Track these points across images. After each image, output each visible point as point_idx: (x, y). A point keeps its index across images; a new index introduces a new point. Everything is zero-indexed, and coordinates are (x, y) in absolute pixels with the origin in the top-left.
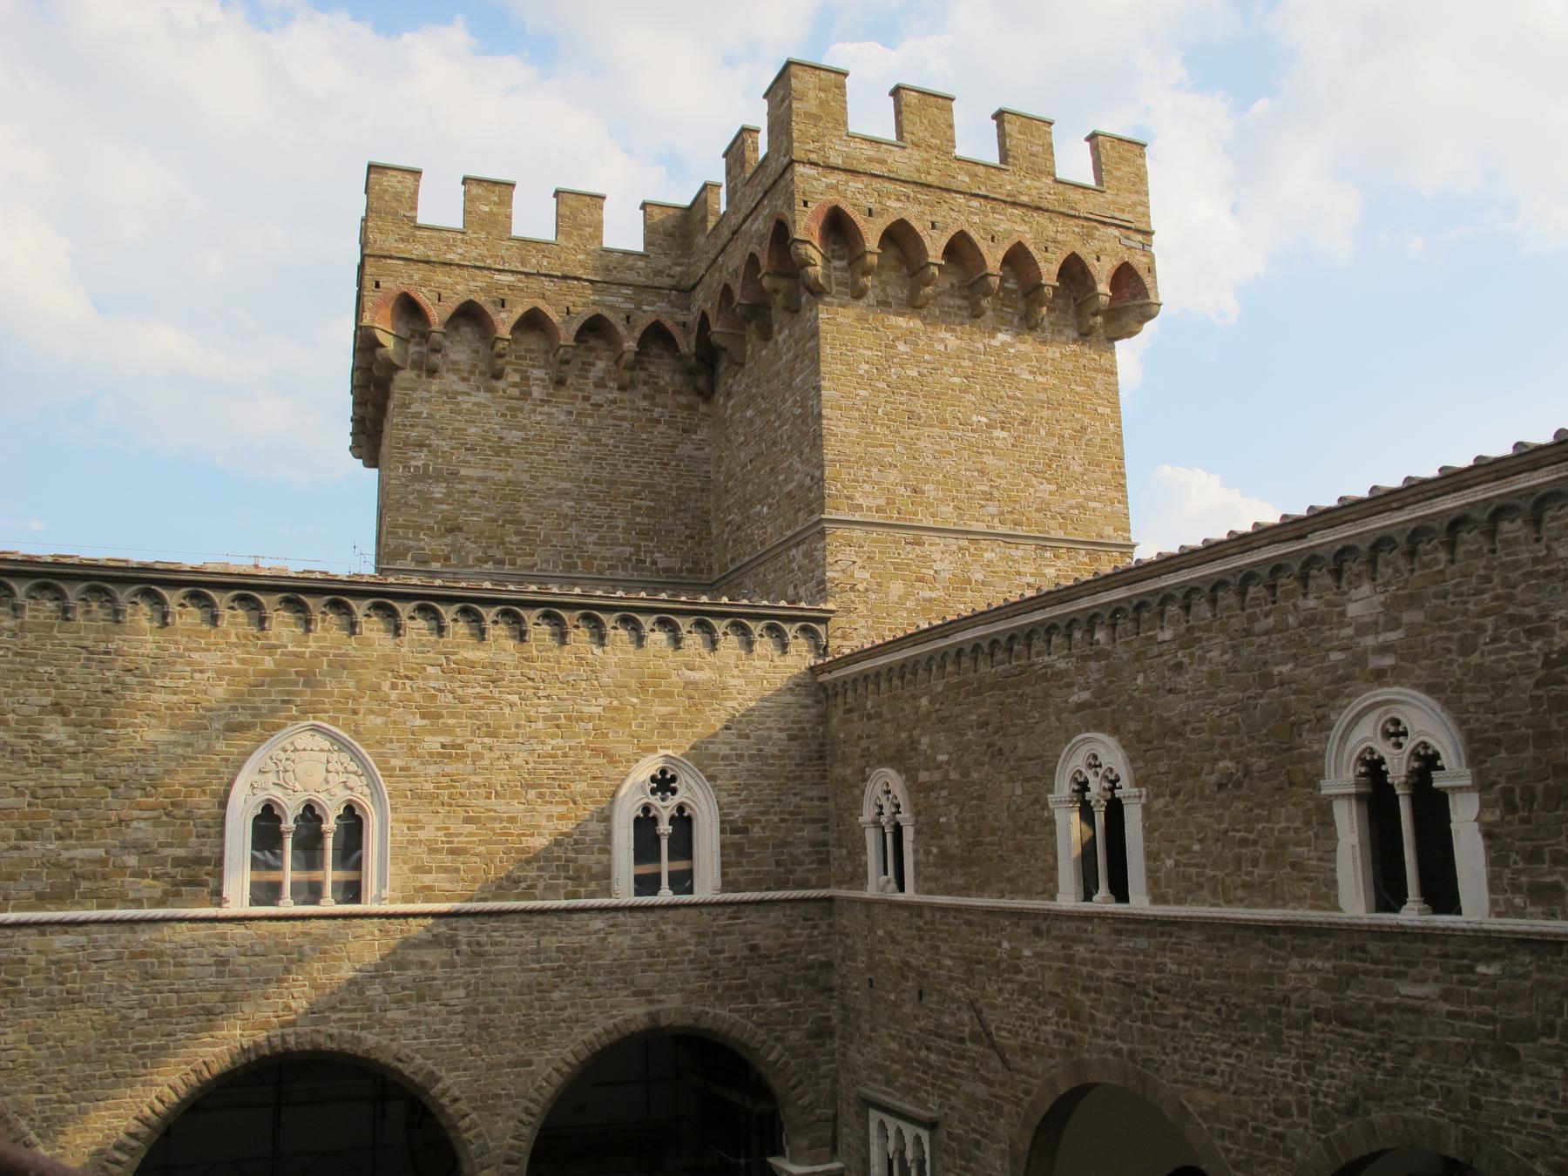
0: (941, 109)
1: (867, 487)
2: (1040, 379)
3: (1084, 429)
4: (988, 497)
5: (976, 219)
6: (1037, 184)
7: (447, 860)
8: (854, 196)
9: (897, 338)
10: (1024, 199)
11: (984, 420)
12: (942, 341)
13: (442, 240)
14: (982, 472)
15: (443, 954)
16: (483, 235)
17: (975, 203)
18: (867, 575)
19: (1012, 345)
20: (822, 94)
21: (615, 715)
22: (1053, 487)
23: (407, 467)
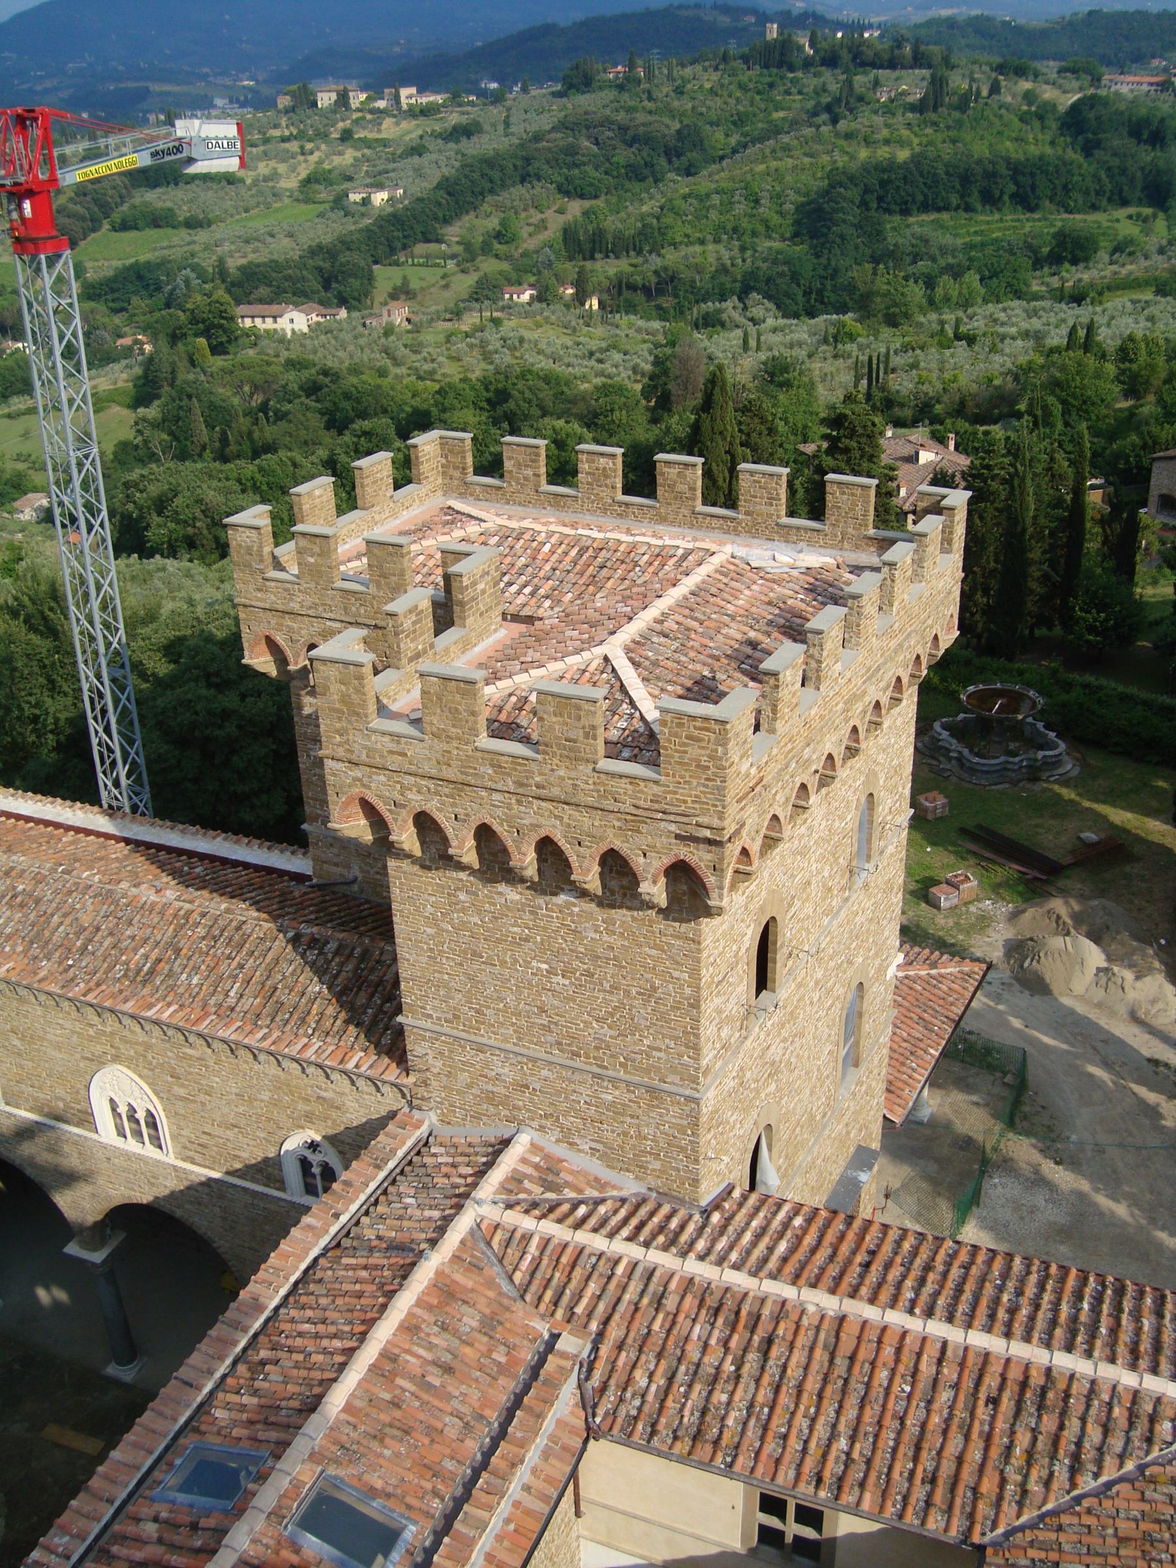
0: (464, 694)
1: (436, 1003)
2: (606, 938)
3: (654, 989)
4: (547, 1029)
5: (499, 812)
6: (573, 774)
7: (199, 1149)
8: (379, 790)
9: (458, 889)
10: (556, 792)
11: (545, 966)
12: (500, 893)
13: (285, 590)
14: (542, 1010)
15: (206, 1190)
16: (313, 585)
17: (496, 796)
18: (439, 1064)
19: (575, 905)
20: (343, 688)
21: (275, 1103)
22: (612, 1033)
23: (309, 756)
